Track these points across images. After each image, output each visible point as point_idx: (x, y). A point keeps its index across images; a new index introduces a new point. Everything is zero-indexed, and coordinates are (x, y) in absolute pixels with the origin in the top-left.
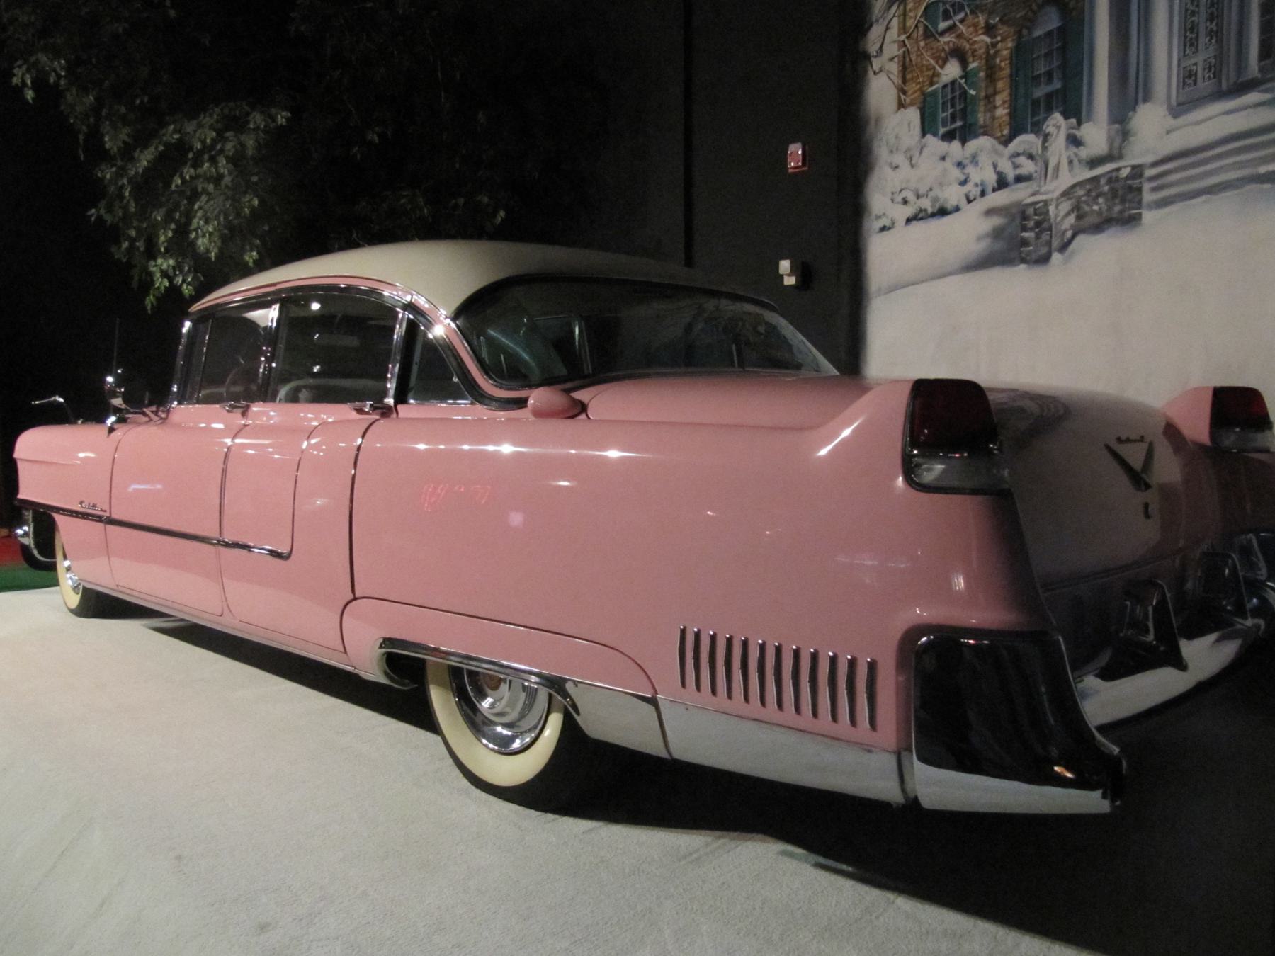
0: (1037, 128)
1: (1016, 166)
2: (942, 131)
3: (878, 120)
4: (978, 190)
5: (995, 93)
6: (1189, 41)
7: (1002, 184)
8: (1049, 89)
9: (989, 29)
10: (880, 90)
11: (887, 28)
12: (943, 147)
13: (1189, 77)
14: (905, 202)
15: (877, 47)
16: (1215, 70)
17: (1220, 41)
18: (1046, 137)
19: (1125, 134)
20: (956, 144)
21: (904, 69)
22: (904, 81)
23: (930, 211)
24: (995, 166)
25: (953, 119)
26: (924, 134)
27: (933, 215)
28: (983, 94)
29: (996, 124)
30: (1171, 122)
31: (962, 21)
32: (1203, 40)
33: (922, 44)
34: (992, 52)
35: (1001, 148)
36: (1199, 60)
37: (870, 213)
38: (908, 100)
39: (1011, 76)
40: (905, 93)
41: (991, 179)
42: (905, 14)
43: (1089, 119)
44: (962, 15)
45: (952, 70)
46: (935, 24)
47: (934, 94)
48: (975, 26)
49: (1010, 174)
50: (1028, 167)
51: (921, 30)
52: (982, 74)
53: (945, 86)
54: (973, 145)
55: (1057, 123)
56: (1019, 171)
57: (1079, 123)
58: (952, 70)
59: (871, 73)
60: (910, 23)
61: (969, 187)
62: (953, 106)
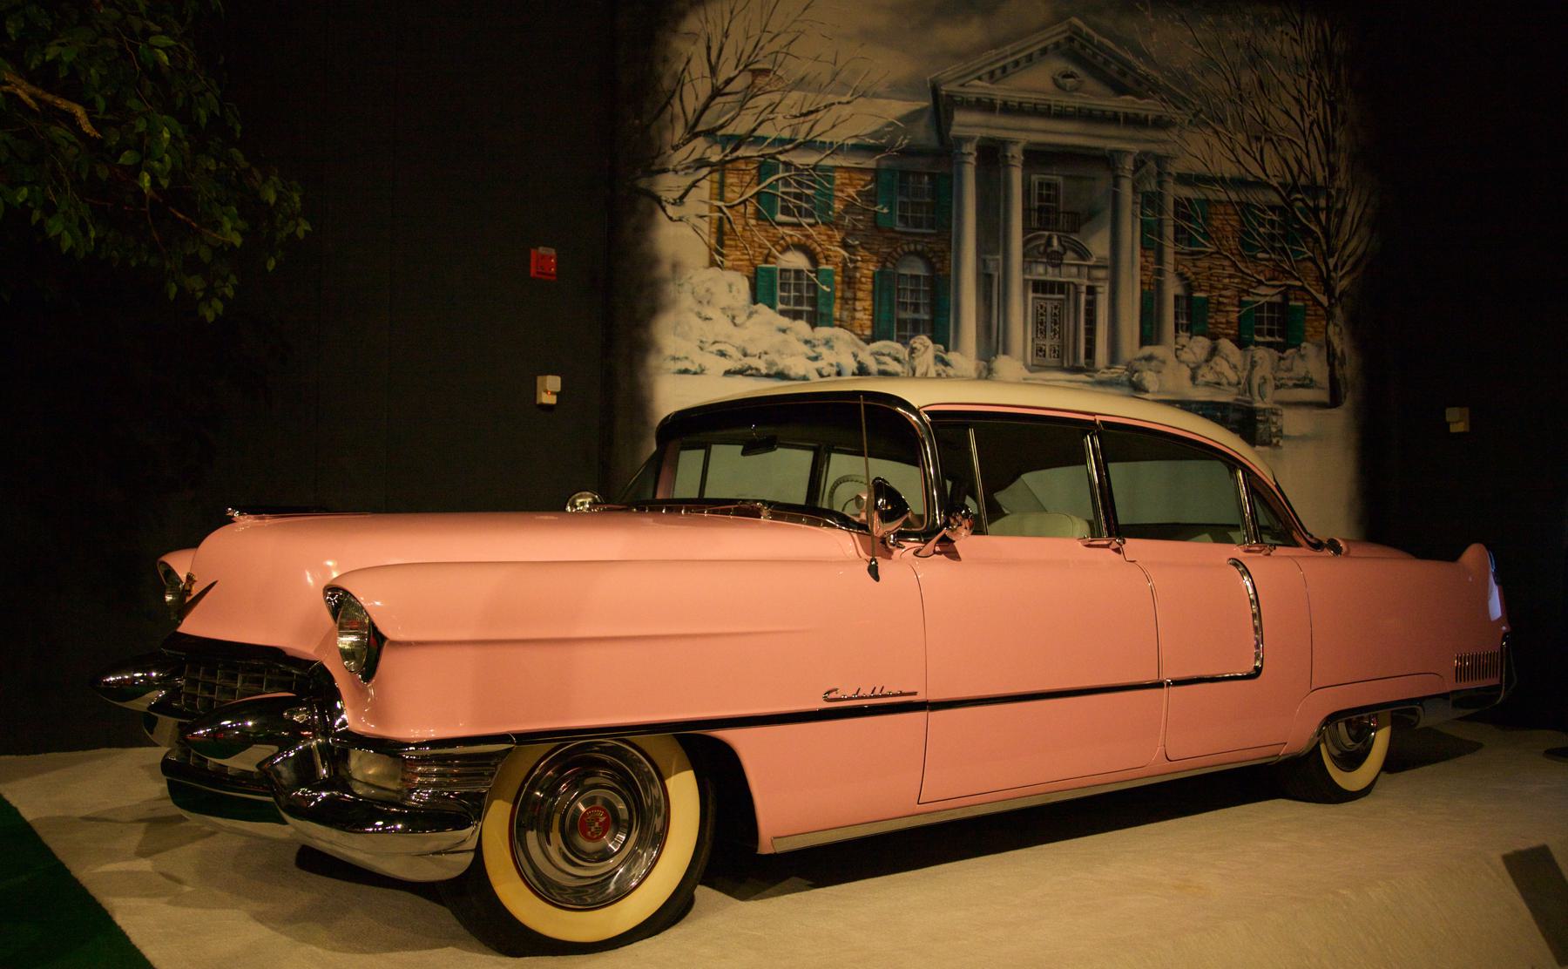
0: (904, 341)
1: (879, 363)
2: (780, 306)
3: (675, 266)
4: (834, 370)
5: (855, 299)
6: (1040, 328)
7: (862, 371)
8: (916, 316)
9: (845, 245)
10: (680, 237)
11: (694, 185)
12: (785, 322)
13: (1040, 351)
14: (722, 354)
15: (677, 195)
16: (1060, 353)
17: (1061, 338)
18: (913, 350)
19: (990, 371)
20: (802, 326)
21: (722, 234)
22: (720, 242)
23: (764, 371)
24: (855, 356)
25: (798, 301)
26: (755, 301)
27: (768, 376)
28: (839, 294)
29: (857, 323)
30: (1026, 373)
31: (810, 225)
32: (1049, 334)
33: (753, 222)
34: (851, 265)
35: (862, 344)
36: (1049, 343)
37: (659, 351)
38: (727, 263)
39: (873, 292)
40: (721, 255)
41: (850, 365)
42: (722, 185)
43: (956, 349)
44: (812, 221)
45: (796, 261)
46: (772, 212)
47: (771, 272)
48: (830, 237)
49: (873, 366)
50: (893, 366)
51: (750, 210)
52: (838, 279)
53: (783, 271)
54: (823, 332)
55: (922, 341)
56: (882, 367)
57: (947, 350)
58: (796, 261)
59: (661, 215)
60: (733, 195)
61: (819, 364)
62: (798, 289)
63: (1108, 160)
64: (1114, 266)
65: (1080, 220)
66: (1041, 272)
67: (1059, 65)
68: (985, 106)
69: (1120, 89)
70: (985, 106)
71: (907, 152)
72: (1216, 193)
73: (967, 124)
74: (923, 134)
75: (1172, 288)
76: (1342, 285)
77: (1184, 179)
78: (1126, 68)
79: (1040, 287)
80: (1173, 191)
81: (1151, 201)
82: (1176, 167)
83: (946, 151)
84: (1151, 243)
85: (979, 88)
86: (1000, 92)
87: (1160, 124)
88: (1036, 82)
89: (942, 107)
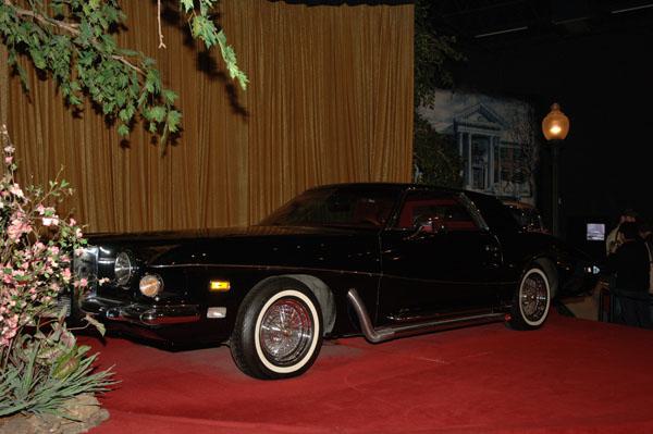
63: (487, 138)
64: (488, 163)
65: (482, 153)
66: (475, 165)
67: (478, 115)
68: (464, 124)
69: (490, 120)
70: (464, 124)
71: (448, 136)
72: (509, 146)
73: (461, 129)
74: (451, 131)
75: (500, 169)
76: (533, 168)
77: (503, 143)
78: (491, 115)
79: (475, 169)
80: (501, 146)
81: (496, 148)
82: (501, 140)
83: (457, 134)
84: (496, 159)
85: (462, 120)
86: (466, 121)
87: (499, 129)
88: (473, 119)
89: (456, 124)
